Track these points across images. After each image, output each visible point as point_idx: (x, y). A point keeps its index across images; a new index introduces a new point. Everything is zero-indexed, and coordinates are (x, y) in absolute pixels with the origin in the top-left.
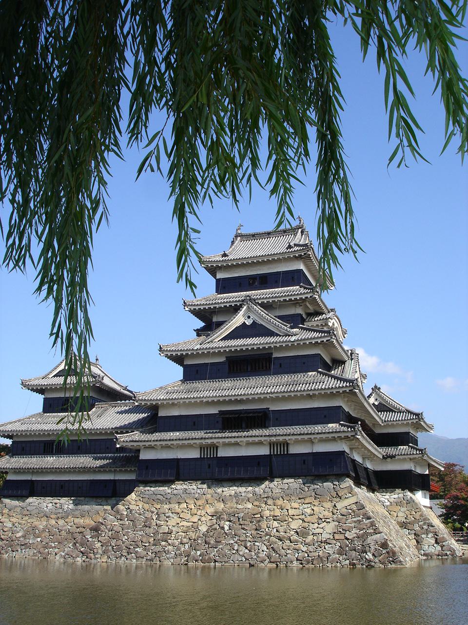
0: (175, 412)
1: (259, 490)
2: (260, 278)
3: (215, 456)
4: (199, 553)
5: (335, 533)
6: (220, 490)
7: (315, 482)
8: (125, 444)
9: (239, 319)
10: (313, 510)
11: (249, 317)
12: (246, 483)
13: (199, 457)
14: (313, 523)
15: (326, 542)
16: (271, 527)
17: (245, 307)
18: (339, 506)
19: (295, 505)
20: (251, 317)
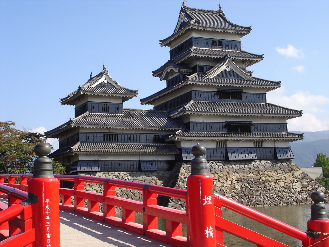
0: (200, 120)
1: (252, 165)
2: (218, 41)
3: (224, 147)
4: (246, 200)
5: (302, 187)
6: (231, 166)
7: (277, 162)
8: (180, 138)
9: (223, 68)
10: (284, 176)
11: (228, 67)
12: (242, 162)
13: (216, 147)
14: (289, 183)
15: (300, 192)
16: (271, 185)
17: (228, 61)
18: (296, 174)
19: (274, 174)
20: (230, 67)
